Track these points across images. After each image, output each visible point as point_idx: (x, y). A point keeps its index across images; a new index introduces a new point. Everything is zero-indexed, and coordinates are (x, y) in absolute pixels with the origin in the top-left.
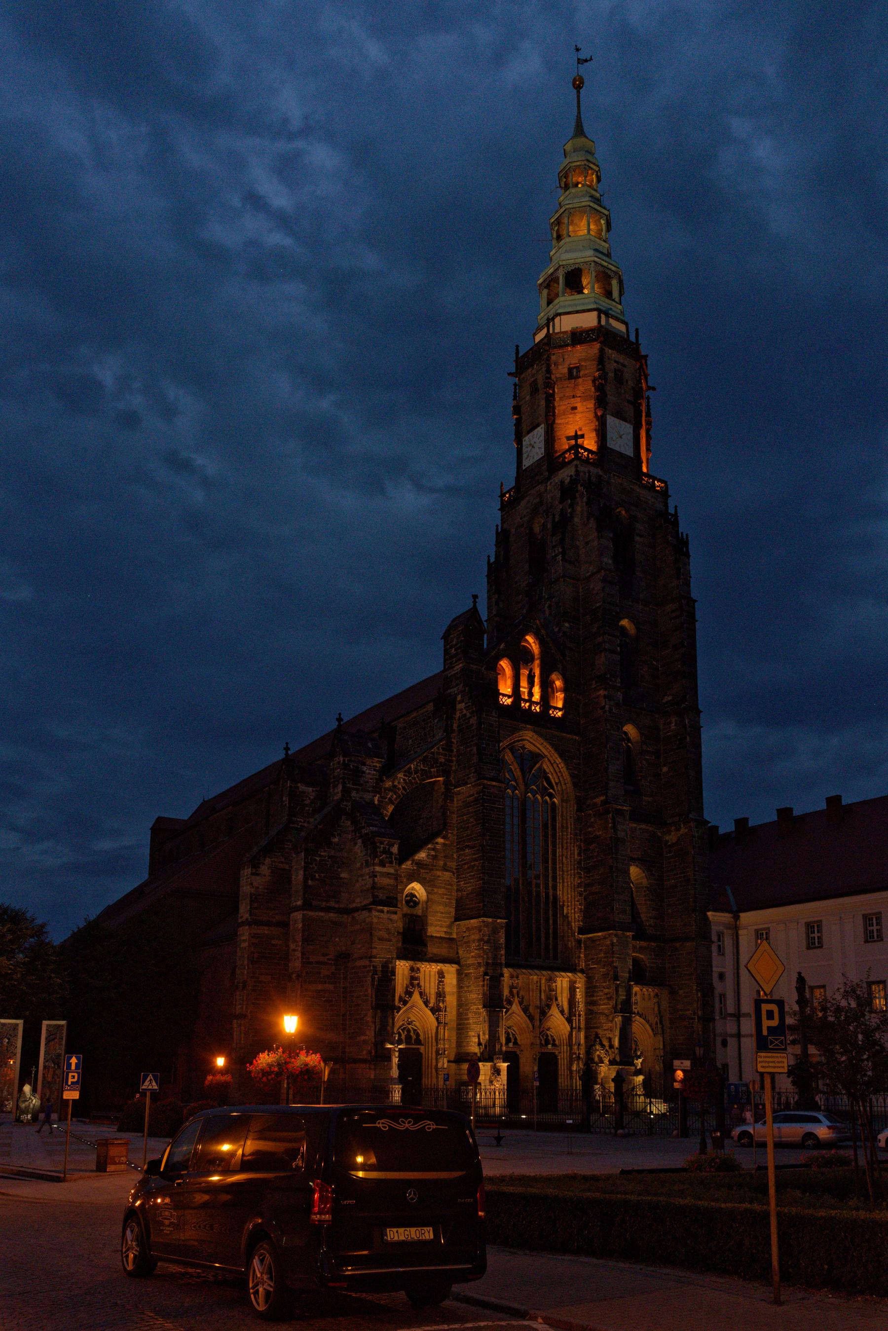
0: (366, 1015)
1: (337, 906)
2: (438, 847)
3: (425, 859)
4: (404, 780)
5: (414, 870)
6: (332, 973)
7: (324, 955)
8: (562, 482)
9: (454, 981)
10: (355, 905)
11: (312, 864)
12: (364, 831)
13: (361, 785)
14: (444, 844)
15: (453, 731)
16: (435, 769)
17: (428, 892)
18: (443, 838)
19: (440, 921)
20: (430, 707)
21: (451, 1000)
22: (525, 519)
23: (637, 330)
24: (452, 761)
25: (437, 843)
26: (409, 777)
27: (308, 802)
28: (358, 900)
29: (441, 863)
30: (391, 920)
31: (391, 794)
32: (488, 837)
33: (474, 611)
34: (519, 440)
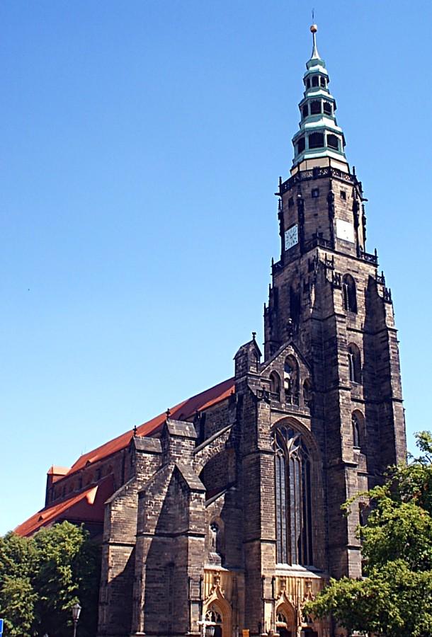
0: (184, 604)
1: (166, 532)
2: (232, 493)
6: (163, 576)
7: (157, 564)
8: (309, 260)
9: (243, 581)
10: (177, 532)
11: (150, 505)
12: (183, 484)
13: (181, 454)
14: (236, 491)
15: (241, 419)
17: (226, 523)
18: (235, 487)
20: (227, 402)
21: (242, 594)
22: (287, 281)
23: (354, 167)
24: (240, 437)
27: (149, 463)
28: (180, 529)
29: (234, 503)
30: (200, 541)
31: (201, 459)
33: (254, 342)
34: (282, 234)
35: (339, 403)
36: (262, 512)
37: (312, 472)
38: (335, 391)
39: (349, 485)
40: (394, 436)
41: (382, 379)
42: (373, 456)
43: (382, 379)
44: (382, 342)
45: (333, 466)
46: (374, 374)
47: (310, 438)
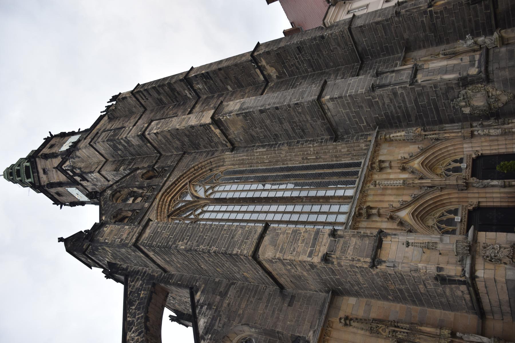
3: (206, 321)
4: (133, 332)
5: (210, 339)
9: (352, 300)
16: (142, 292)
19: (274, 311)
25: (199, 301)
26: (134, 326)
32: (180, 243)
35: (157, 133)
36: (214, 248)
37: (237, 168)
38: (148, 137)
39: (240, 109)
40: (220, 69)
41: (176, 94)
42: (246, 94)
43: (176, 94)
44: (147, 99)
45: (227, 137)
46: (176, 105)
47: (197, 170)
